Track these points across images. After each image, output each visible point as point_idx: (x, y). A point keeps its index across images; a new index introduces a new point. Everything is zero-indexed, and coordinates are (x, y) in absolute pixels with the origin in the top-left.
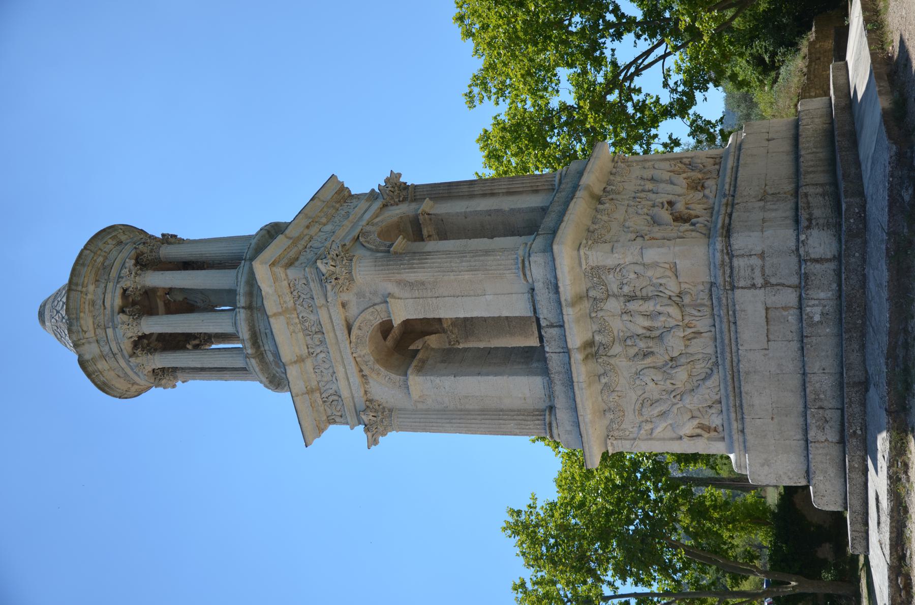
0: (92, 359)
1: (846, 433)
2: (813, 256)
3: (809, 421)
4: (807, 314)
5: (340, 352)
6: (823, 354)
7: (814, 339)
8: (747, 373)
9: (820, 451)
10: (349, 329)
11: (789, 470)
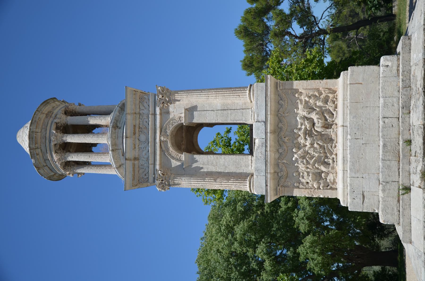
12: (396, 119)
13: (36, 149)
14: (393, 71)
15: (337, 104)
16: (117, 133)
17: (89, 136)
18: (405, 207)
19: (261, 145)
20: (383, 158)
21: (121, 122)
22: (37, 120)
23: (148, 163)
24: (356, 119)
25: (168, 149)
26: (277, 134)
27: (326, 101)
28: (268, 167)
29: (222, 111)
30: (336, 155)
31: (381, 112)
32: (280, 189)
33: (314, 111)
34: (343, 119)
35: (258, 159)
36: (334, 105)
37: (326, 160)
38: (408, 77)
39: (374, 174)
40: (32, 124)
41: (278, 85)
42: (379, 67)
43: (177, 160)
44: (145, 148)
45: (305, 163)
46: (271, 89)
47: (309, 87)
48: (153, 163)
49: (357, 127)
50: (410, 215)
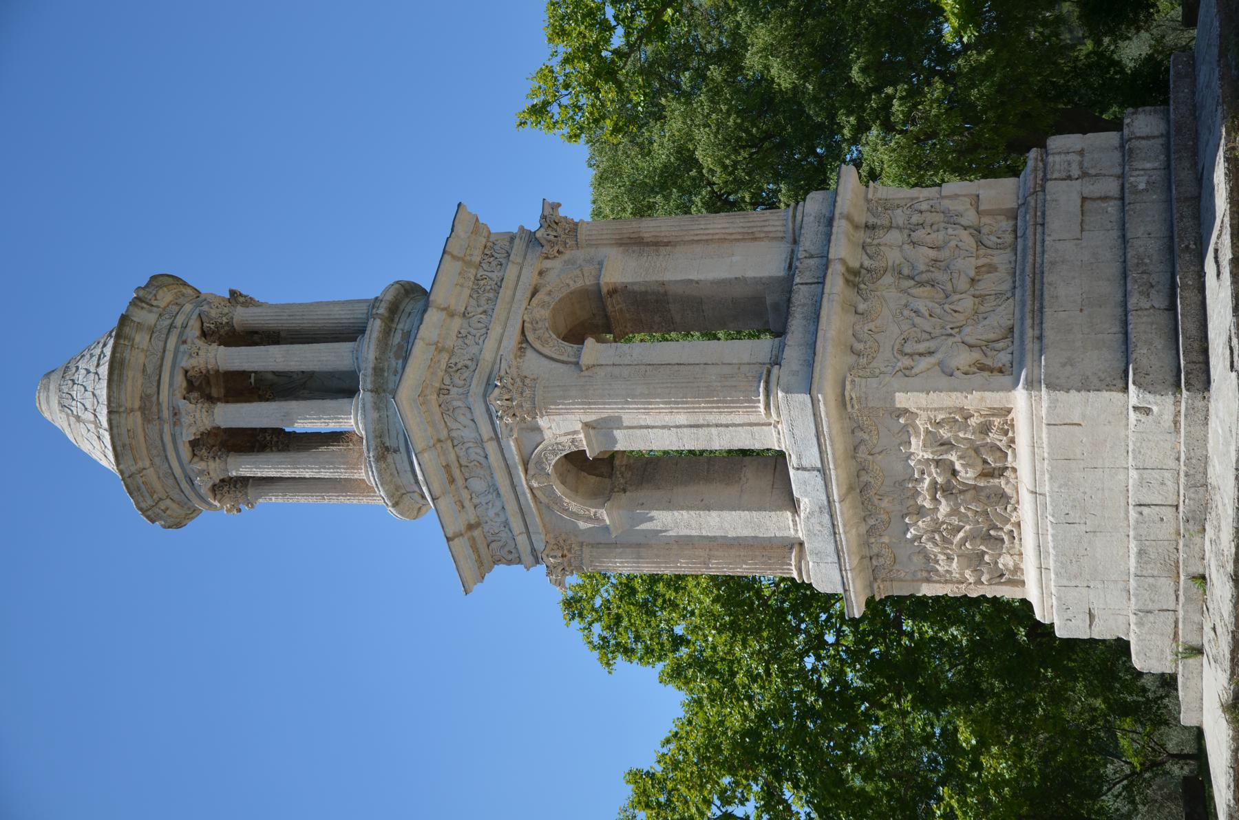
0: (139, 323)
1: (1176, 247)
2: (1138, 135)
3: (1129, 288)
4: (1131, 183)
5: (509, 313)
6: (1148, 219)
7: (1138, 206)
8: (1053, 263)
9: (1144, 319)
10: (534, 293)
11: (1100, 370)
12: (1170, 508)
13: (157, 503)
14: (1161, 422)
15: (1014, 437)
16: (392, 466)
17: (309, 468)
18: (1190, 676)
19: (817, 509)
20: (1139, 573)
21: (393, 433)
22: (127, 442)
23: (509, 532)
24: (1068, 489)
25: (557, 501)
26: (858, 491)
27: (985, 429)
28: (845, 562)
29: (694, 430)
30: (1018, 525)
31: (1133, 495)
32: (879, 588)
33: (952, 450)
34: (1033, 481)
35: (815, 535)
36: (1005, 438)
37: (992, 532)
38: (1201, 470)
39: (1116, 582)
40: (120, 458)
41: (848, 403)
42: (1126, 395)
43: (588, 519)
44: (490, 504)
45: (939, 543)
46: (829, 421)
47: (935, 406)
48: (524, 530)
49: (1070, 504)
50: (1200, 689)
